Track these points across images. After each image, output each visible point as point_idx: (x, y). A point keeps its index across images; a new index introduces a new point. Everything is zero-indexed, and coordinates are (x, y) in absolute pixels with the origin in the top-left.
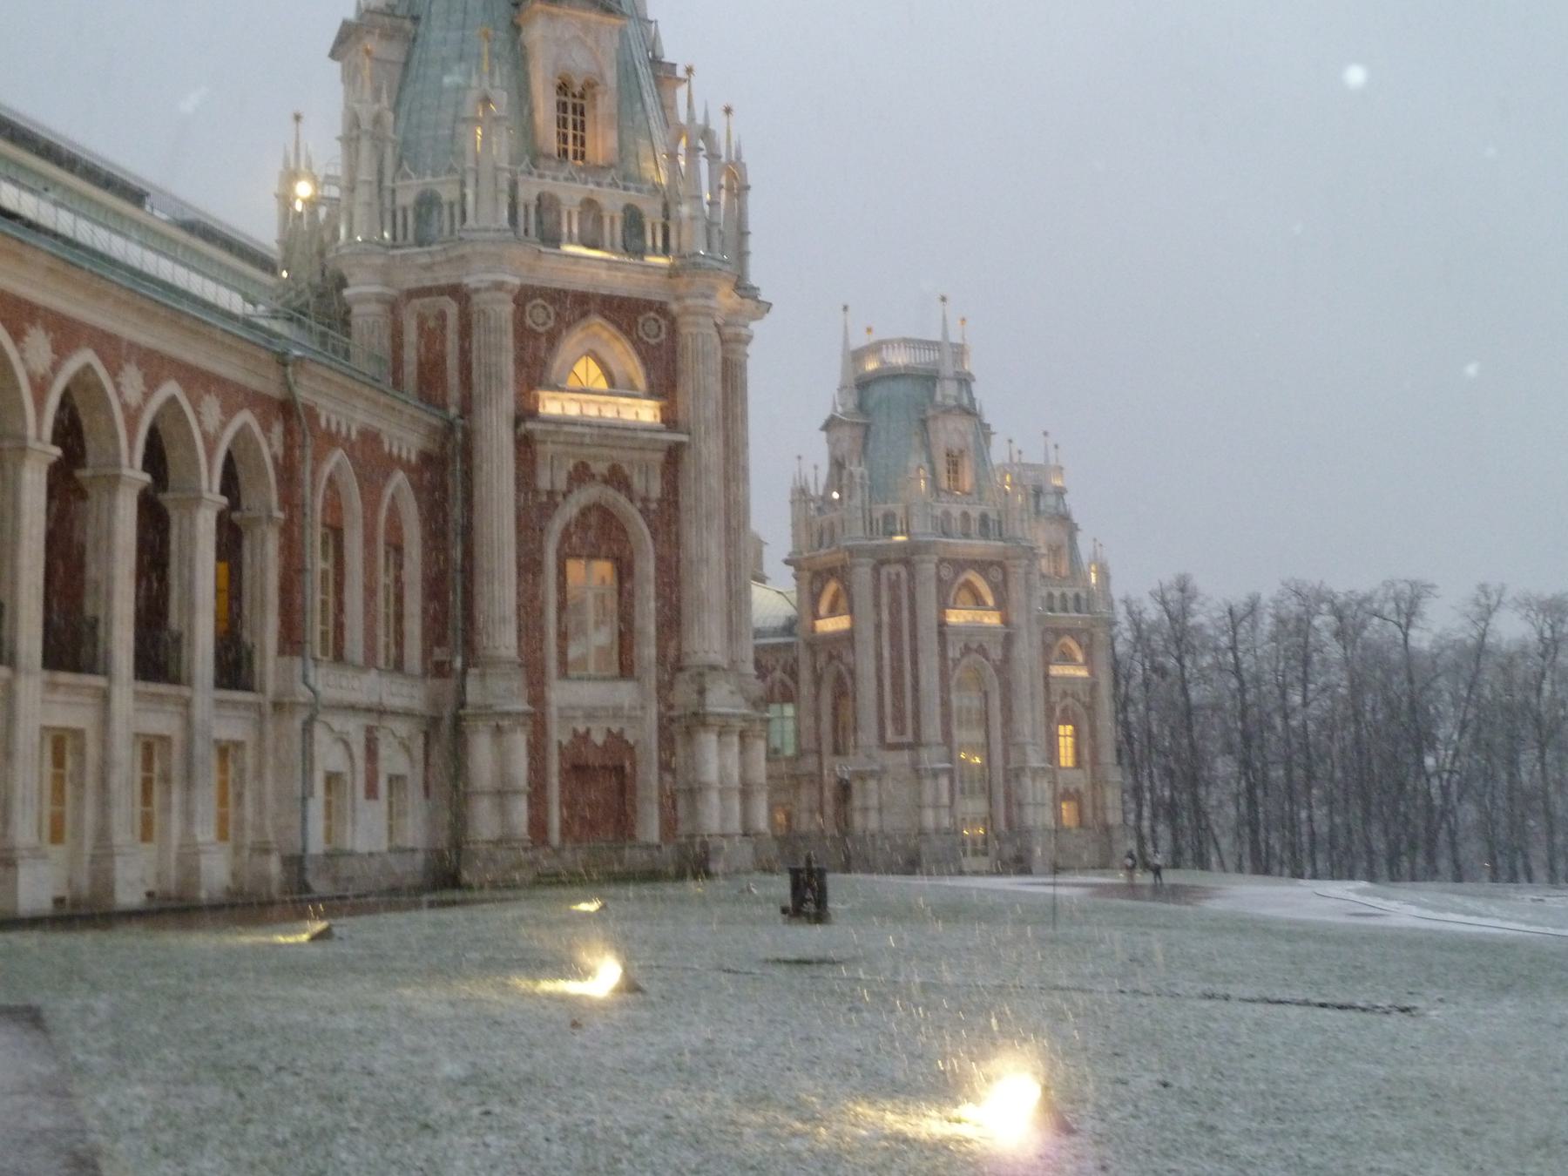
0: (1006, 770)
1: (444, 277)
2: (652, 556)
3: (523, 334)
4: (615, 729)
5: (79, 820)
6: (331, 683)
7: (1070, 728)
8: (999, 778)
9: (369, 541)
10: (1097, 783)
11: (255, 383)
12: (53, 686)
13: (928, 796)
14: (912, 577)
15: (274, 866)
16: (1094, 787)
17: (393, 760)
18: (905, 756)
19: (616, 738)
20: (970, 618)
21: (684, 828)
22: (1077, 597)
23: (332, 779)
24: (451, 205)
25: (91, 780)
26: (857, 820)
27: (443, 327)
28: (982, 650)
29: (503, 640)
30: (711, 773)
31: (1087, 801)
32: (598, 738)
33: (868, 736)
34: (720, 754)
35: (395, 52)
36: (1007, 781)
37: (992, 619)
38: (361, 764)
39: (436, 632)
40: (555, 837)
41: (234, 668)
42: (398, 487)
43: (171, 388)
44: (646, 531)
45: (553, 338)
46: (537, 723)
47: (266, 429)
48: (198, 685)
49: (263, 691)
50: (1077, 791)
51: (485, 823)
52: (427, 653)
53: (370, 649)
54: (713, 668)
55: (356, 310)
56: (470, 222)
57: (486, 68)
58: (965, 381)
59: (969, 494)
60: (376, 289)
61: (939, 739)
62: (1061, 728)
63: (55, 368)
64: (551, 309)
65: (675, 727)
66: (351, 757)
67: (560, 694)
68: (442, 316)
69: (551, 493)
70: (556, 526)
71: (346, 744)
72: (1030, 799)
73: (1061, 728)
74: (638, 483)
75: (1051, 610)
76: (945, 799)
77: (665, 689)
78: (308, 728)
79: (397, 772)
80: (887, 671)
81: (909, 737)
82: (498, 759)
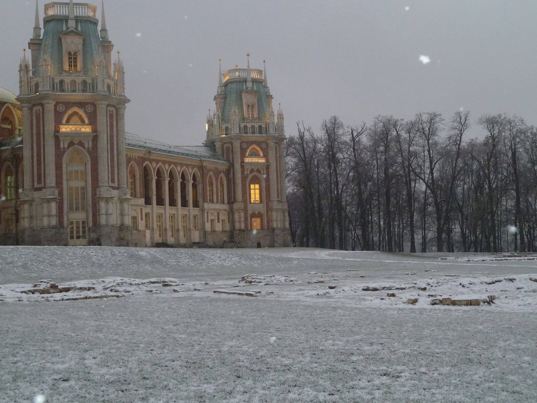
7: (257, 186)
10: (269, 209)
13: (45, 211)
14: (43, 110)
20: (73, 129)
22: (260, 127)
28: (81, 144)
31: (265, 217)
37: (87, 129)
59: (80, 72)
61: (54, 184)
62: (252, 186)
72: (103, 211)
73: (252, 186)
75: (246, 133)
76: (54, 211)
80: (35, 154)
81: (42, 185)
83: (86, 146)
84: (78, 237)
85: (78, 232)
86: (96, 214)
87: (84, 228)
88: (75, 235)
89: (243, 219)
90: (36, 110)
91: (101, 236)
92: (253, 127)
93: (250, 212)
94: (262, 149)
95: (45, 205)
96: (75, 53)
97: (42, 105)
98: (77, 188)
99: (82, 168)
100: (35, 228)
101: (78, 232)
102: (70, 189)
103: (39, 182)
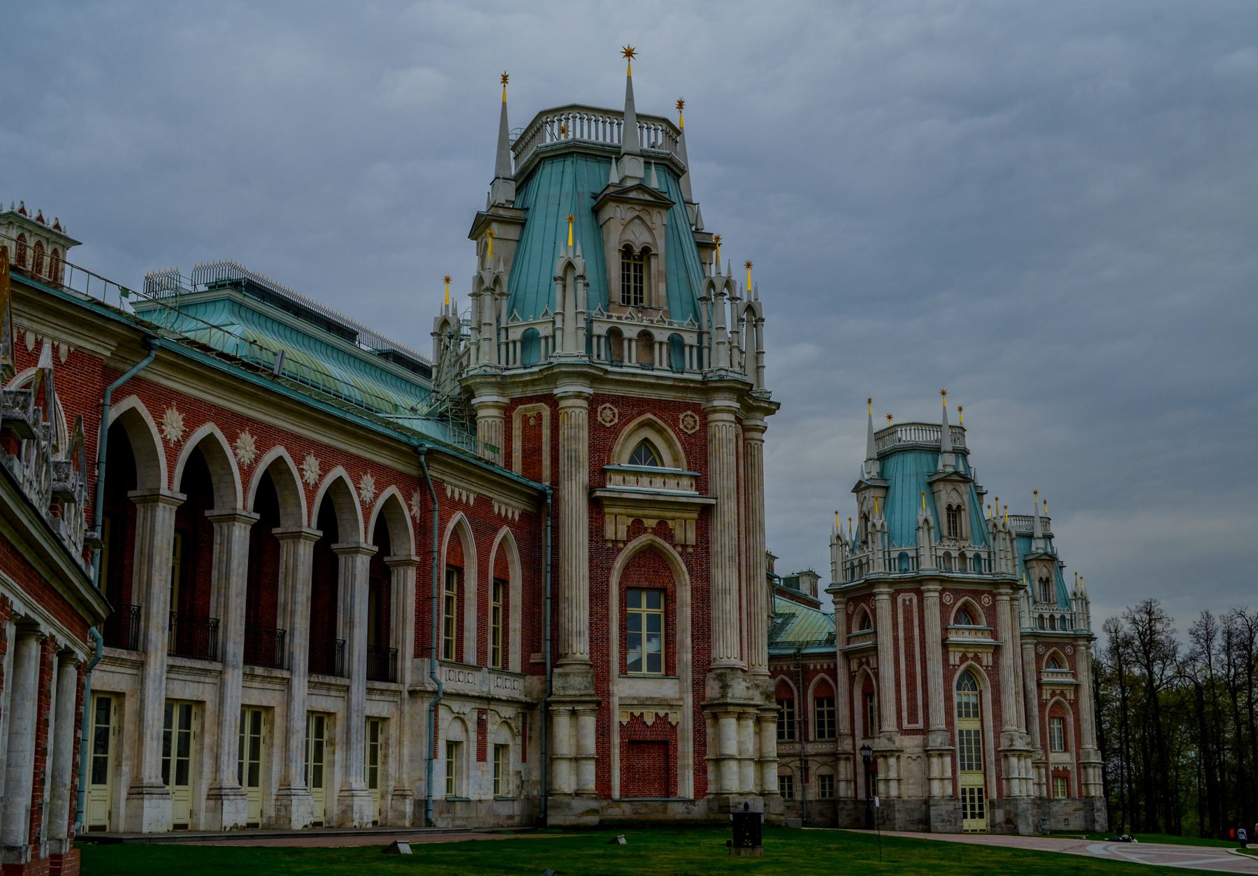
0: (997, 752)
1: (541, 390)
2: (689, 587)
3: (595, 427)
4: (662, 713)
5: (269, 769)
6: (449, 679)
8: (991, 757)
9: (482, 574)
11: (400, 467)
12: (253, 676)
13: (935, 772)
15: (408, 807)
16: (1078, 768)
17: (497, 734)
18: (918, 739)
19: (662, 720)
21: (711, 788)
23: (452, 746)
24: (546, 338)
25: (278, 740)
26: (881, 787)
27: (540, 425)
29: (580, 648)
30: (731, 748)
31: (1074, 775)
32: (650, 720)
33: (890, 724)
34: (738, 733)
35: (512, 232)
36: (998, 760)
38: (473, 736)
39: (531, 642)
40: (616, 794)
41: (382, 665)
42: (505, 538)
43: (339, 471)
44: (684, 569)
45: (615, 431)
46: (602, 708)
47: (408, 498)
48: (355, 677)
49: (403, 682)
50: (1065, 769)
51: (565, 779)
52: (525, 659)
53: (481, 653)
54: (733, 669)
55: (481, 413)
56: (558, 350)
57: (570, 243)
58: (963, 453)
60: (495, 398)
61: (944, 727)
63: (257, 459)
64: (616, 411)
65: (707, 712)
66: (467, 731)
67: (622, 689)
68: (539, 417)
69: (616, 541)
70: (619, 564)
71: (463, 721)
74: (679, 535)
76: (949, 774)
77: (699, 686)
78: (434, 710)
79: (502, 742)
81: (920, 725)
82: (574, 735)
83: (985, 663)
84: (973, 816)
85: (973, 807)
86: (1003, 778)
87: (980, 799)
88: (969, 811)
89: (1044, 780)
90: (904, 601)
91: (1016, 815)
92: (1052, 617)
93: (1052, 768)
94: (1067, 656)
95: (935, 761)
96: (959, 507)
97: (920, 594)
98: (968, 732)
99: (973, 700)
100: (905, 797)
101: (973, 807)
102: (961, 732)
103: (913, 718)
